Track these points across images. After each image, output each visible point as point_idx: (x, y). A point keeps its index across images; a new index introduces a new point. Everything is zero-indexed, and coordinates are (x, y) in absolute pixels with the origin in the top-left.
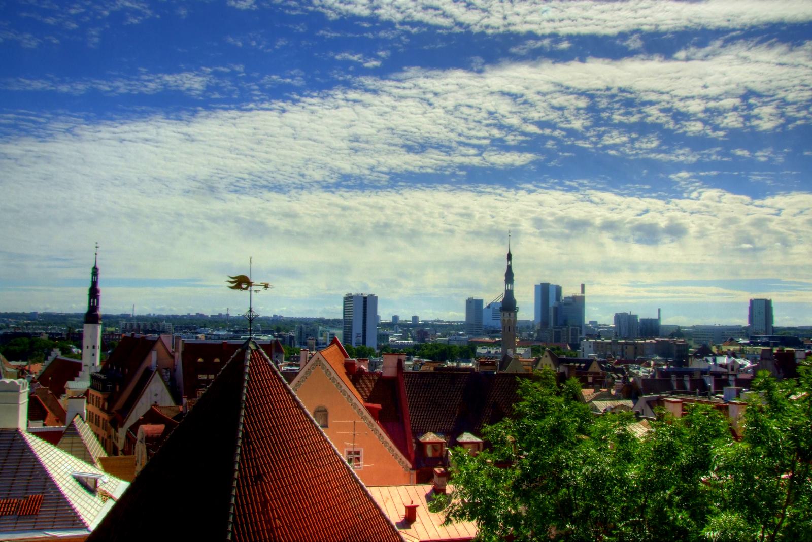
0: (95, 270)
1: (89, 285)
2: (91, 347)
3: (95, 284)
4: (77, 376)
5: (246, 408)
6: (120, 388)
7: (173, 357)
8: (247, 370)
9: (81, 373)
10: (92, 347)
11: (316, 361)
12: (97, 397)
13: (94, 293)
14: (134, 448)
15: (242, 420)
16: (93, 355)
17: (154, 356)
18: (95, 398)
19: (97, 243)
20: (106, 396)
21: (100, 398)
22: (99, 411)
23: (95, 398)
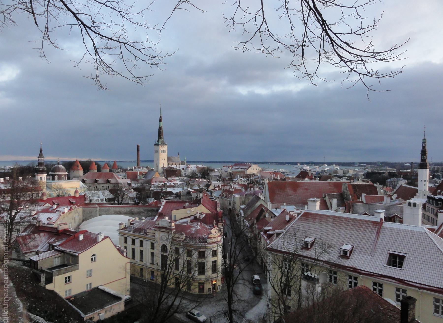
1: (421, 148)
3: (424, 147)
4: (416, 196)
9: (417, 194)
10: (424, 181)
12: (432, 208)
13: (424, 152)
16: (425, 185)
18: (430, 209)
19: (424, 126)
21: (434, 209)
23: (430, 209)
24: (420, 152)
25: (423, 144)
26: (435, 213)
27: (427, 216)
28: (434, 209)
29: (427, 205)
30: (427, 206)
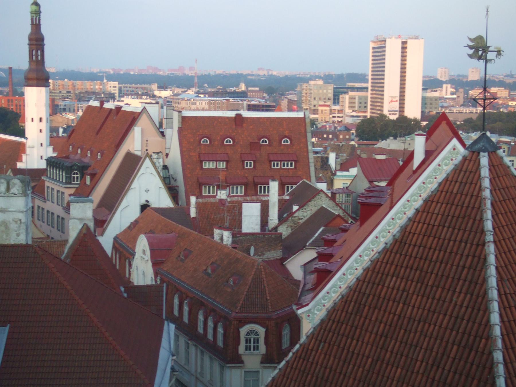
0: (34, 7)
1: (28, 29)
2: (37, 120)
3: (36, 26)
4: (21, 161)
5: (495, 242)
6: (91, 180)
7: (162, 134)
8: (486, 183)
9: (24, 157)
10: (39, 120)
11: (450, 152)
12: (58, 191)
14: (130, 265)
15: (492, 259)
16: (41, 131)
17: (137, 132)
18: (55, 192)
20: (72, 191)
21: (63, 193)
22: (63, 211)
23: (55, 192)
24: (27, 41)
25: (32, 20)
26: (65, 205)
27: (48, 211)
28: (63, 193)
29: (47, 184)
30: (48, 187)
